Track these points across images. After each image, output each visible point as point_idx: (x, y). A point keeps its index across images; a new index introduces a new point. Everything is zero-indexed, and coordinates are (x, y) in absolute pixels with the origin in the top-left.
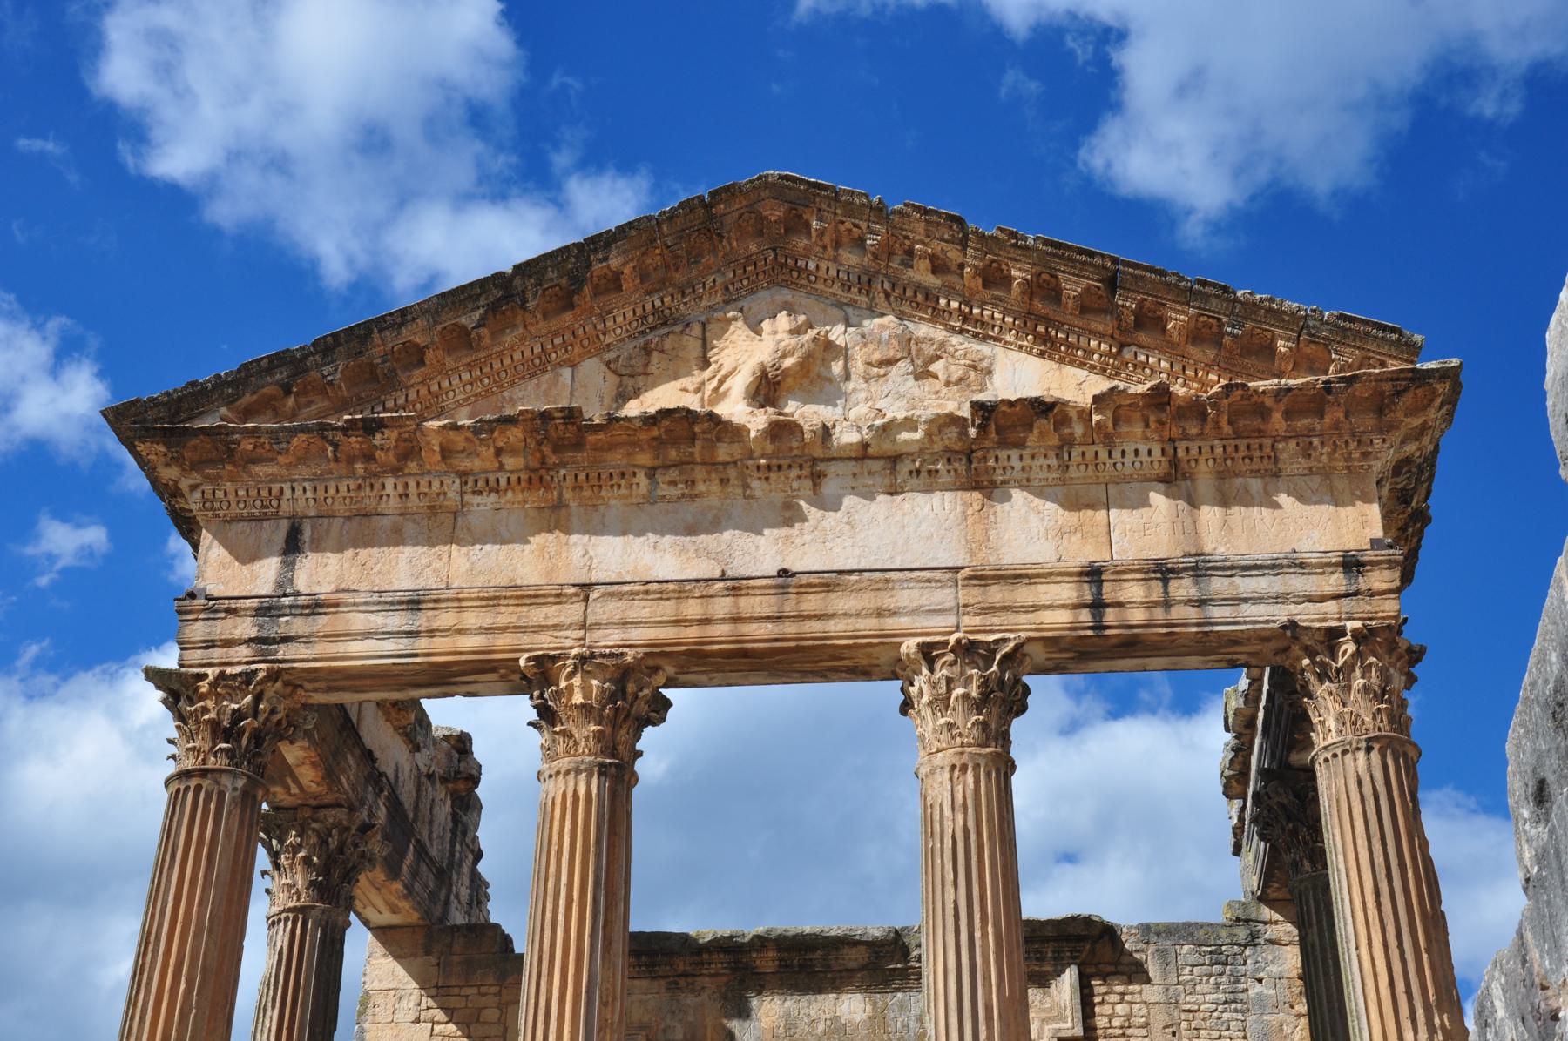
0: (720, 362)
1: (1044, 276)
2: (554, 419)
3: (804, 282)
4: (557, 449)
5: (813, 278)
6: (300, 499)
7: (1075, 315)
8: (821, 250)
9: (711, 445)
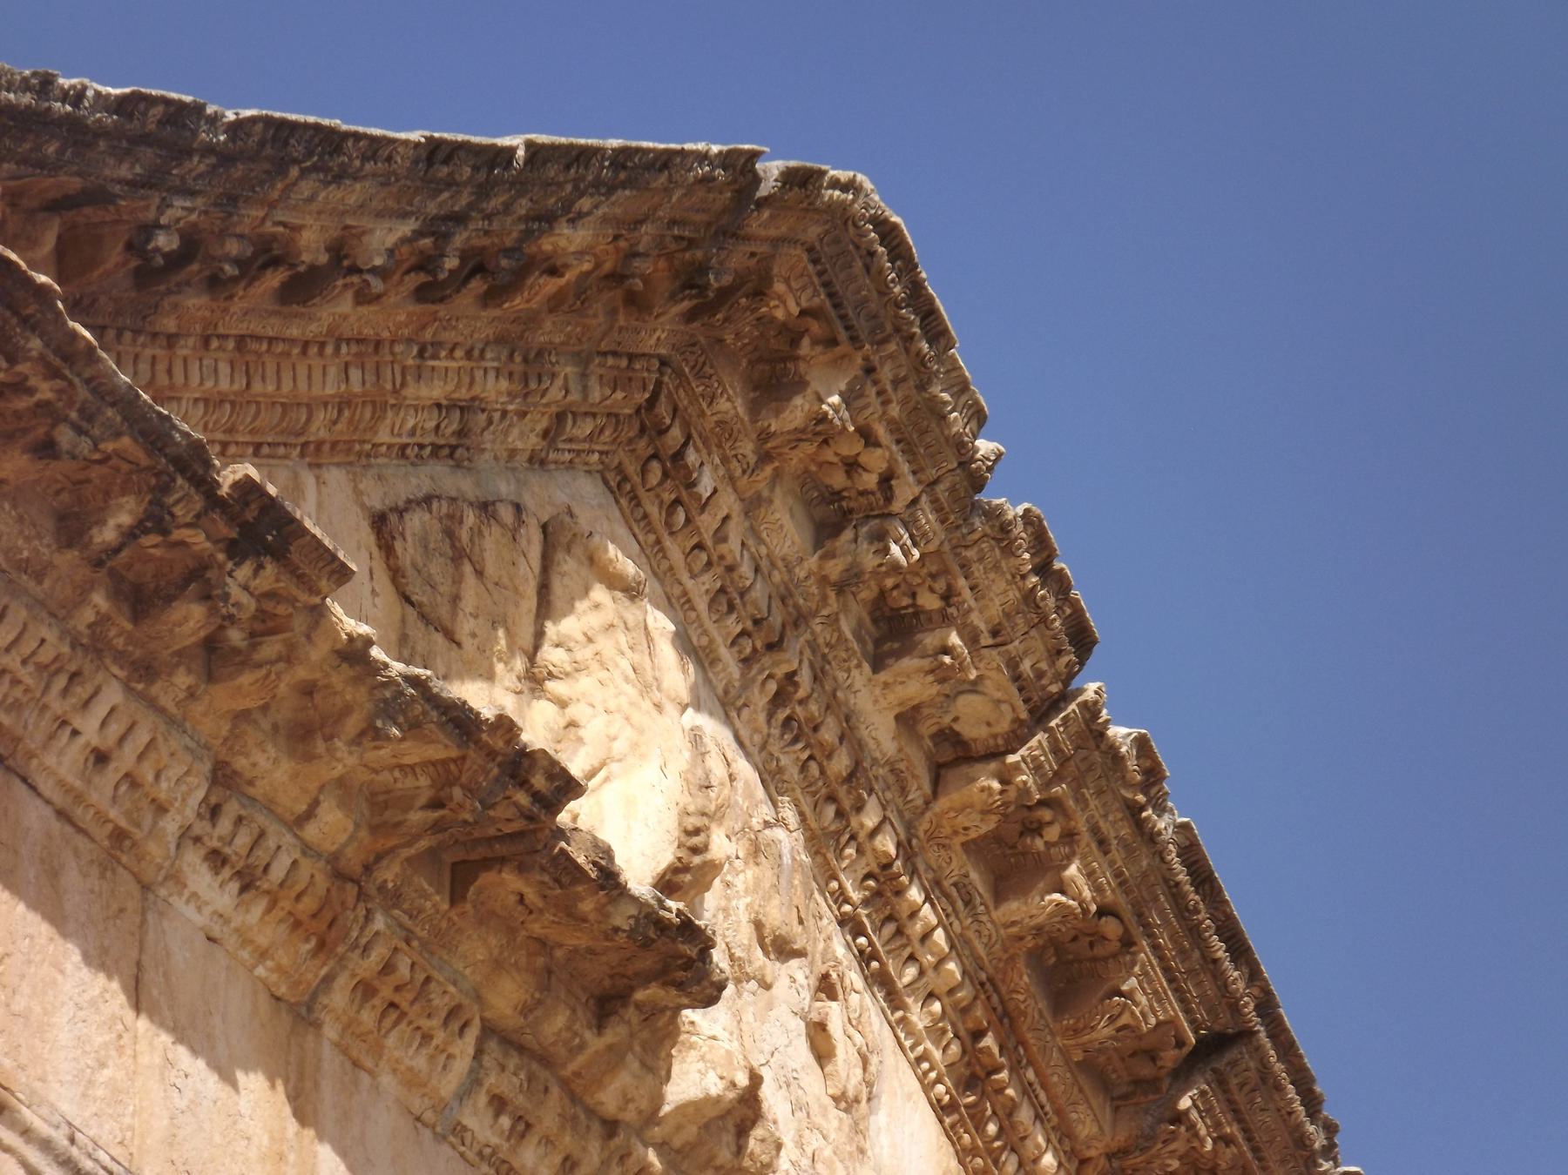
0: (573, 711)
1: (1111, 927)
2: (524, 784)
3: (653, 510)
5: (681, 516)
7: (1067, 1061)
8: (752, 459)
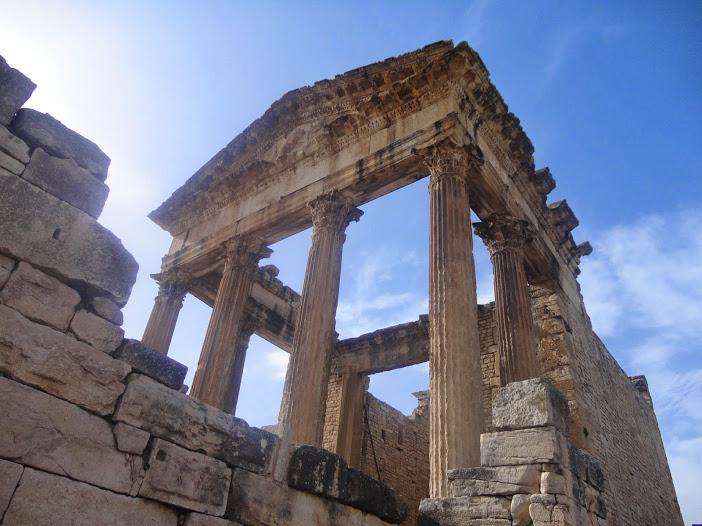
4: (235, 188)
6: (188, 225)
9: (268, 171)
